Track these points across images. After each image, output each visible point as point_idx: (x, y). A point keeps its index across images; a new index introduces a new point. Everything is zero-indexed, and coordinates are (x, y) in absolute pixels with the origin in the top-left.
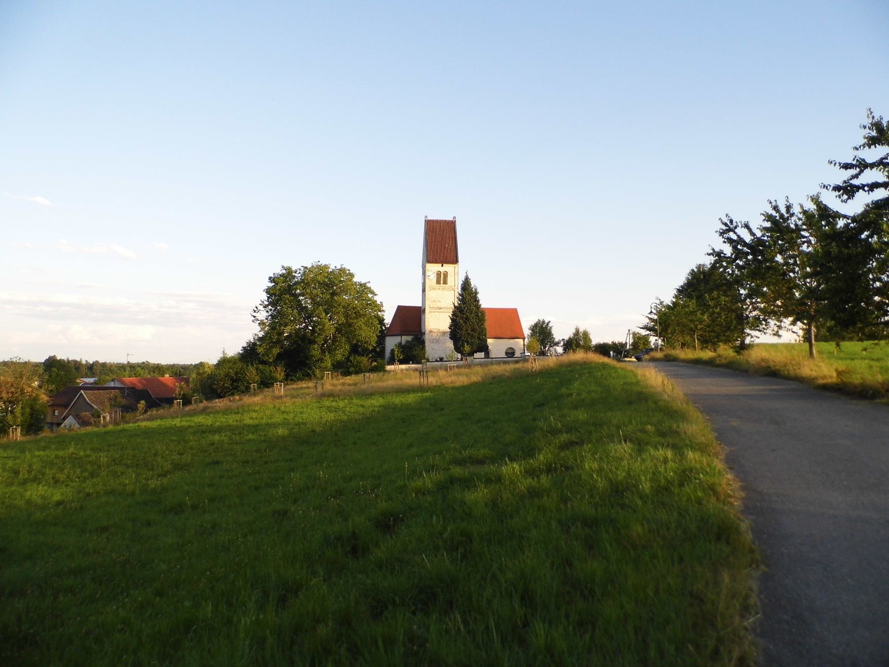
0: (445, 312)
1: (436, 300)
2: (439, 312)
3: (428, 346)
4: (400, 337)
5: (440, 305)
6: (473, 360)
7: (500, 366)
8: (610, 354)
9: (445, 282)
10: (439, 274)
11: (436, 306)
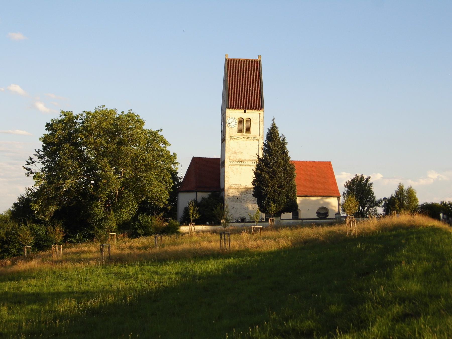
0: (247, 165)
1: (238, 151)
2: (241, 165)
4: (195, 194)
6: (280, 222)
7: (312, 228)
8: (439, 216)
9: (248, 131)
10: (241, 121)
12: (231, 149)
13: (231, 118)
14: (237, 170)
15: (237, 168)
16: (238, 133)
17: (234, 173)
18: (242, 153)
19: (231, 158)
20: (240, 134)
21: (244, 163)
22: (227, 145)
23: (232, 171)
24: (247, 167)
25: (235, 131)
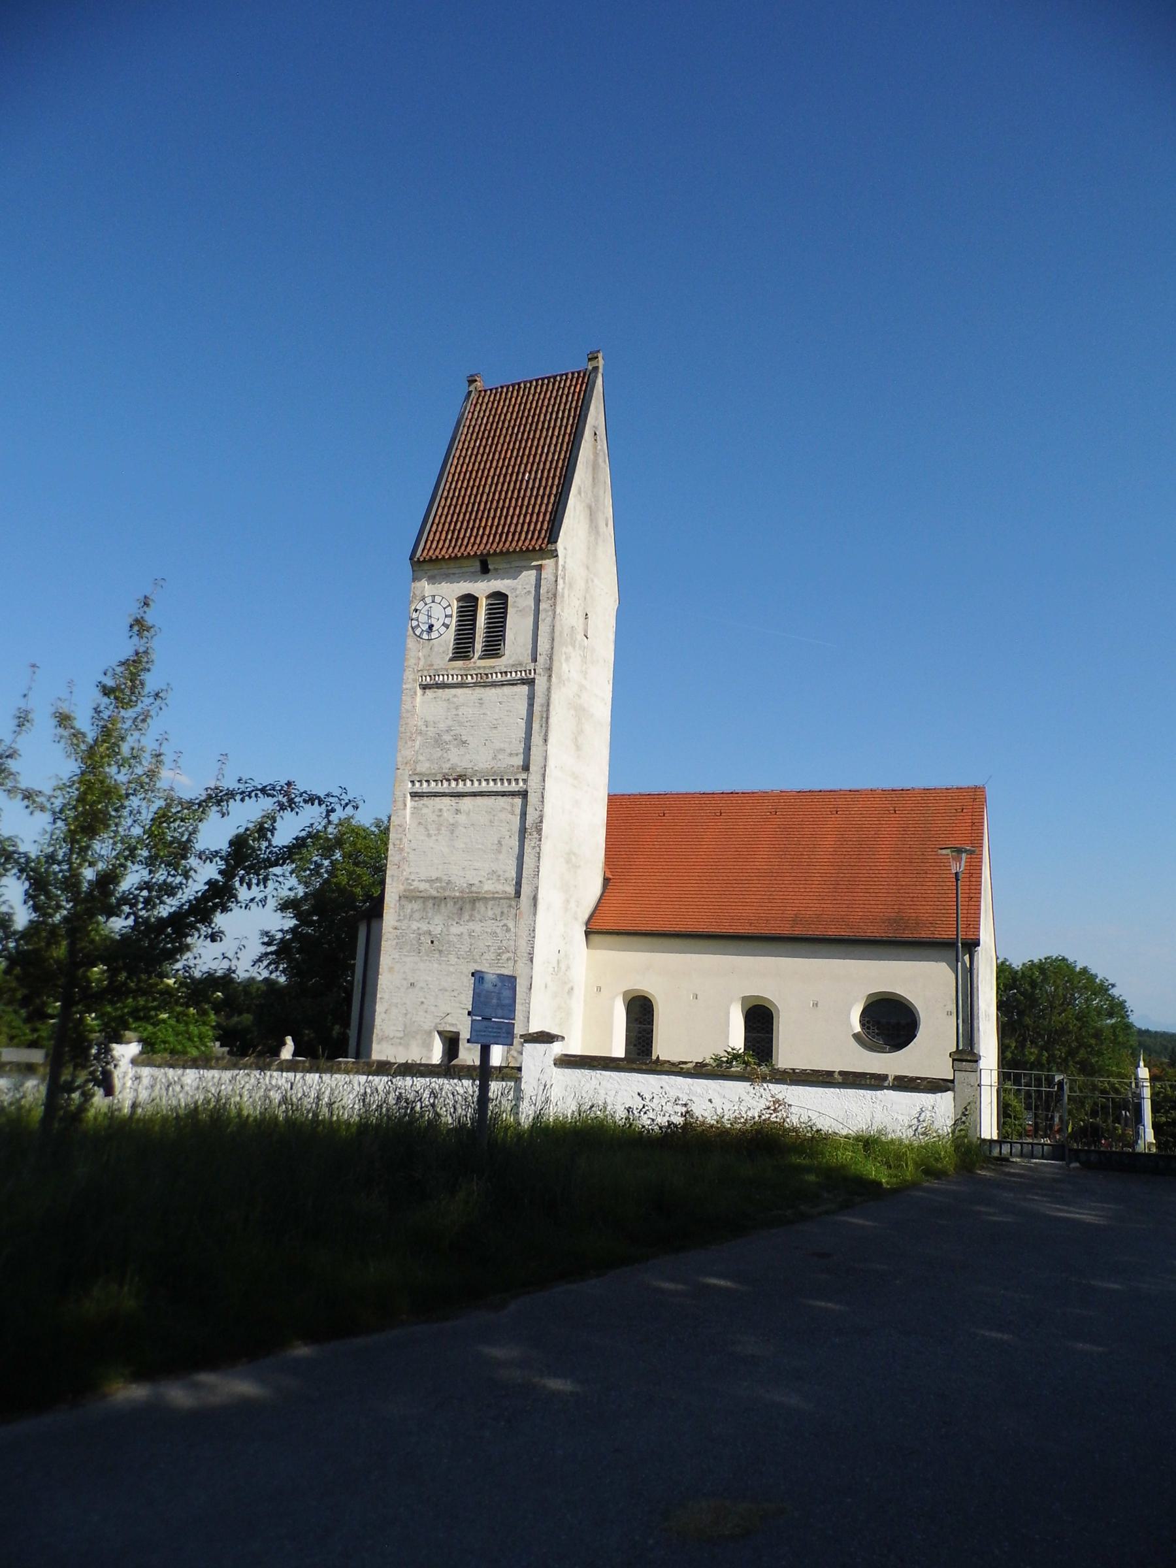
0: (481, 794)
1: (447, 737)
3: (391, 969)
5: (457, 759)
9: (494, 647)
10: (468, 603)
11: (446, 767)
12: (424, 728)
13: (429, 600)
14: (440, 816)
15: (441, 810)
16: (451, 660)
17: (427, 829)
18: (464, 742)
19: (423, 767)
20: (459, 663)
21: (468, 783)
22: (408, 711)
23: (420, 823)
24: (479, 800)
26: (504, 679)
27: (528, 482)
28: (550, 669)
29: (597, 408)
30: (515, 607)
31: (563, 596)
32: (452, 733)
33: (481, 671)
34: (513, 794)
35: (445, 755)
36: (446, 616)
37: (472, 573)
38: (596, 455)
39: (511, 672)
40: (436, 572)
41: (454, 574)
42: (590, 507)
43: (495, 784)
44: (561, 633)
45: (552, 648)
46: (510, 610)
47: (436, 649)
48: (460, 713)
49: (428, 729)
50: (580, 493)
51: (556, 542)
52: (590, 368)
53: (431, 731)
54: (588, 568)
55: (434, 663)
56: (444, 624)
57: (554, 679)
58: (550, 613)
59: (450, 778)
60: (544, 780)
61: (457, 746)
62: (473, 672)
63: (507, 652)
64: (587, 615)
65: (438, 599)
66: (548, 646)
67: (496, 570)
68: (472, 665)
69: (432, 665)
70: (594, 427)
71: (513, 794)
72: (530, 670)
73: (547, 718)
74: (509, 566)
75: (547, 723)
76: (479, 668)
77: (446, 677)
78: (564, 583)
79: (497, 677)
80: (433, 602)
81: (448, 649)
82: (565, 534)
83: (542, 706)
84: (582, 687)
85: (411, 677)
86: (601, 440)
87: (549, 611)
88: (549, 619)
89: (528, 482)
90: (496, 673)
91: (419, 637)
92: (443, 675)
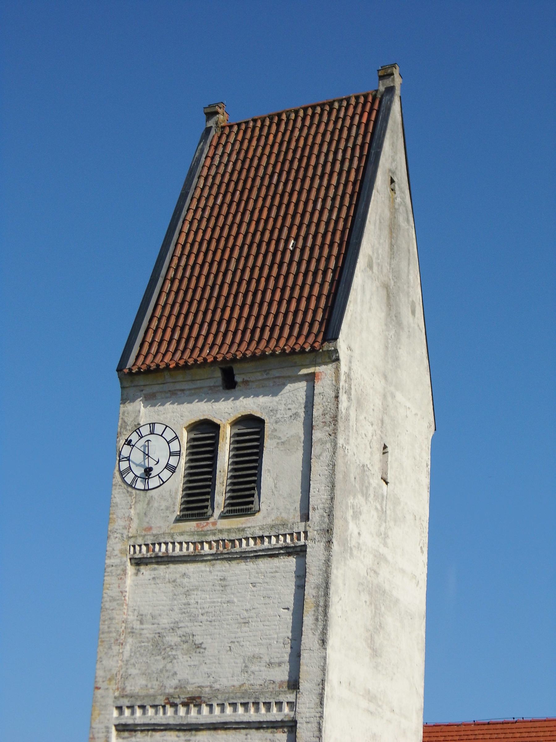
1: (172, 639)
11: (170, 685)
12: (137, 625)
13: (145, 430)
16: (179, 520)
20: (191, 525)
21: (205, 710)
22: (113, 599)
25: (167, 508)
26: (259, 547)
27: (293, 253)
28: (329, 531)
29: (393, 144)
30: (275, 437)
31: (347, 419)
32: (180, 632)
33: (225, 536)
34: (273, 725)
35: (169, 666)
36: (171, 454)
37: (210, 388)
38: (394, 211)
39: (269, 537)
40: (156, 388)
41: (183, 390)
42: (386, 287)
43: (247, 710)
44: (346, 475)
45: (332, 499)
46: (269, 443)
47: (156, 505)
48: (192, 601)
49: (144, 626)
50: (370, 266)
51: (336, 338)
52: (382, 89)
53: (148, 630)
54: (385, 377)
55: (153, 525)
56: (168, 467)
57: (335, 547)
58: (328, 445)
59: (177, 701)
60: (321, 704)
61: (187, 652)
62: (211, 538)
63: (263, 507)
64: (385, 447)
65: (159, 429)
66: (325, 496)
67: (246, 382)
68: (210, 527)
69: (150, 529)
70: (390, 170)
71: (273, 725)
72: (299, 533)
73: (326, 606)
74: (265, 376)
75: (325, 614)
76: (221, 531)
77: (170, 546)
78: (349, 399)
79: (248, 544)
80: (152, 433)
81: (174, 504)
82: (349, 326)
83: (318, 587)
84: (380, 558)
85: (119, 547)
86: (401, 189)
87: (326, 442)
88: (326, 457)
89: (293, 253)
90: (247, 539)
91: (130, 486)
92: (166, 544)
